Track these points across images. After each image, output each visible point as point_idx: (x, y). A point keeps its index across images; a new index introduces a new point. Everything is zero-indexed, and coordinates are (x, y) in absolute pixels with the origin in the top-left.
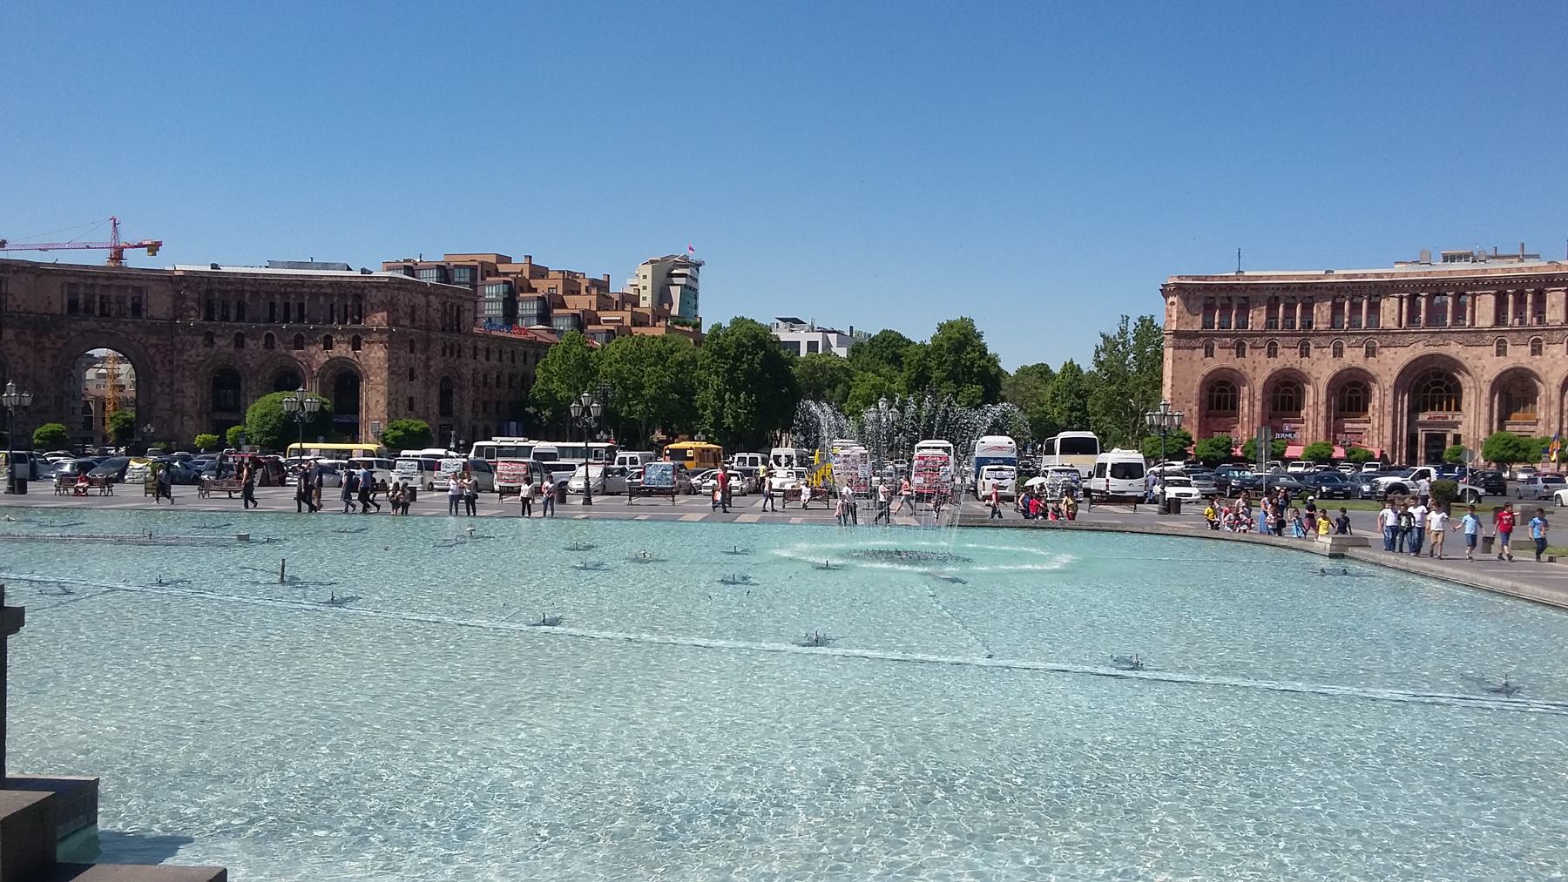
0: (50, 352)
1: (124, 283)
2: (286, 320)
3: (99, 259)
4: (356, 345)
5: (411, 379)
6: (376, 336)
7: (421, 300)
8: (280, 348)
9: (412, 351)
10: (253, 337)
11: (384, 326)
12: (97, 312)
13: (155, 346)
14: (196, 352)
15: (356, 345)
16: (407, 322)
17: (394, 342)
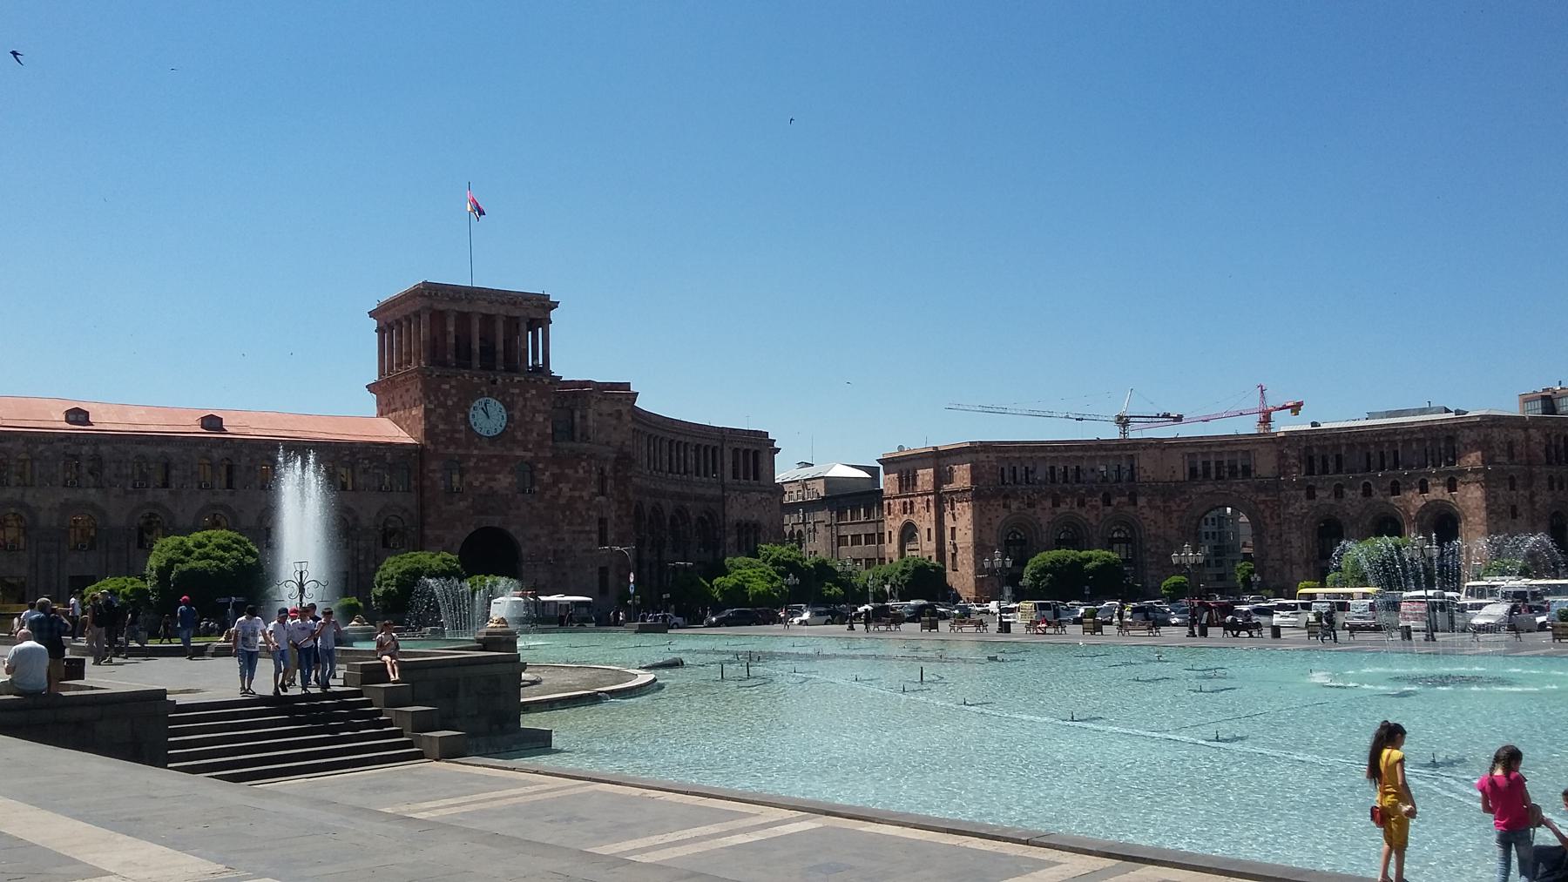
0: (1175, 515)
1: (1234, 448)
2: (1382, 469)
3: (1248, 426)
4: (1452, 486)
5: (1514, 516)
6: (1471, 477)
7: (1519, 435)
8: (1377, 496)
9: (1512, 488)
10: (1351, 487)
11: (1479, 465)
12: (1213, 476)
13: (1264, 502)
14: (1299, 505)
15: (1452, 486)
16: (1504, 459)
17: (1489, 482)
